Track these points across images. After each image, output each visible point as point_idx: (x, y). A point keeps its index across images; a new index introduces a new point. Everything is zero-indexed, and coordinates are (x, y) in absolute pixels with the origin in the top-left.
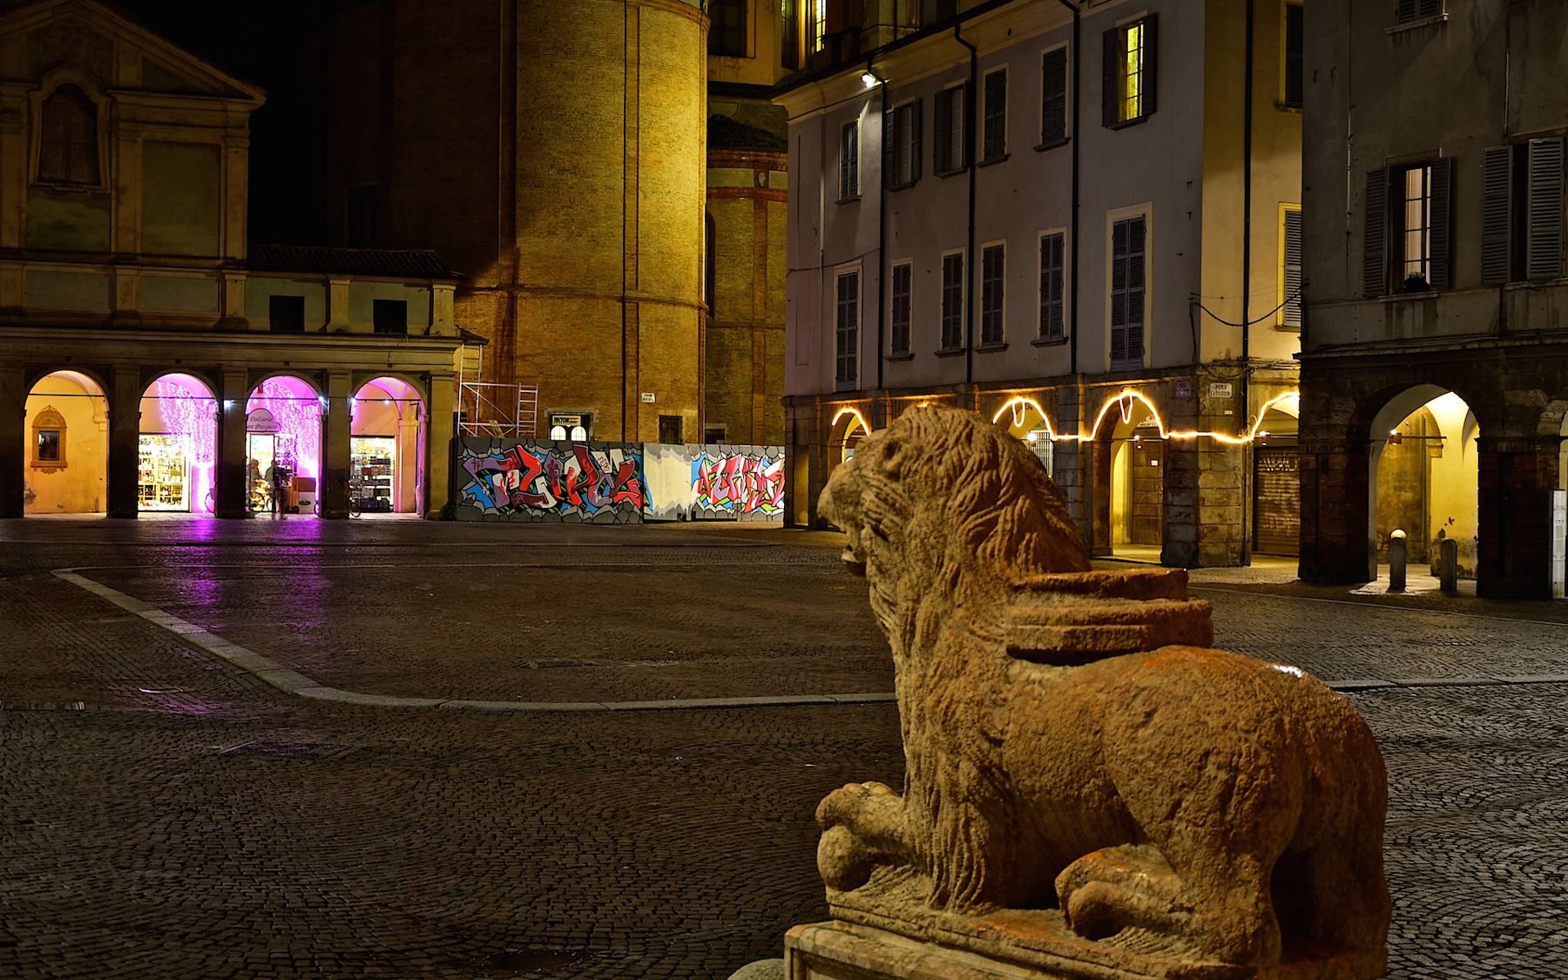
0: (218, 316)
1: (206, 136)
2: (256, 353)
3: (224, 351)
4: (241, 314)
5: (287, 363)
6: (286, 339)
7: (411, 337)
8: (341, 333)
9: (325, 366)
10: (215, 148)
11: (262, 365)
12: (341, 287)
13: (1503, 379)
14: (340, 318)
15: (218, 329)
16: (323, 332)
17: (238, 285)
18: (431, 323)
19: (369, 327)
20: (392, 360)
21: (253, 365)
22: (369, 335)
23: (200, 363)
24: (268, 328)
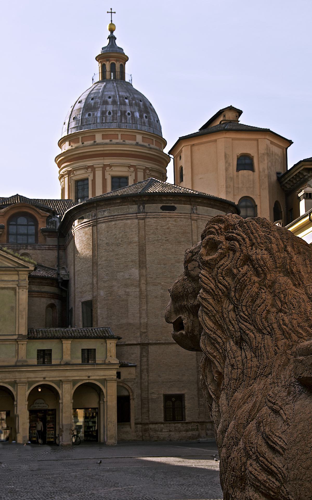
0: (15, 360)
1: (10, 285)
2: (32, 375)
3: (17, 375)
4: (24, 358)
5: (44, 378)
6: (44, 368)
7: (97, 364)
8: (67, 364)
9: (61, 379)
10: (14, 289)
11: (34, 379)
12: (67, 344)
13: (192, 302)
14: (67, 358)
15: (16, 366)
16: (60, 365)
17: (23, 347)
18: (106, 358)
19: (80, 361)
20: (90, 374)
21: (30, 380)
22: (80, 364)
23: (7, 380)
24: (36, 364)
